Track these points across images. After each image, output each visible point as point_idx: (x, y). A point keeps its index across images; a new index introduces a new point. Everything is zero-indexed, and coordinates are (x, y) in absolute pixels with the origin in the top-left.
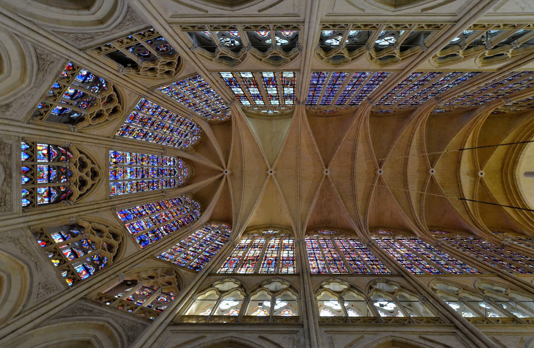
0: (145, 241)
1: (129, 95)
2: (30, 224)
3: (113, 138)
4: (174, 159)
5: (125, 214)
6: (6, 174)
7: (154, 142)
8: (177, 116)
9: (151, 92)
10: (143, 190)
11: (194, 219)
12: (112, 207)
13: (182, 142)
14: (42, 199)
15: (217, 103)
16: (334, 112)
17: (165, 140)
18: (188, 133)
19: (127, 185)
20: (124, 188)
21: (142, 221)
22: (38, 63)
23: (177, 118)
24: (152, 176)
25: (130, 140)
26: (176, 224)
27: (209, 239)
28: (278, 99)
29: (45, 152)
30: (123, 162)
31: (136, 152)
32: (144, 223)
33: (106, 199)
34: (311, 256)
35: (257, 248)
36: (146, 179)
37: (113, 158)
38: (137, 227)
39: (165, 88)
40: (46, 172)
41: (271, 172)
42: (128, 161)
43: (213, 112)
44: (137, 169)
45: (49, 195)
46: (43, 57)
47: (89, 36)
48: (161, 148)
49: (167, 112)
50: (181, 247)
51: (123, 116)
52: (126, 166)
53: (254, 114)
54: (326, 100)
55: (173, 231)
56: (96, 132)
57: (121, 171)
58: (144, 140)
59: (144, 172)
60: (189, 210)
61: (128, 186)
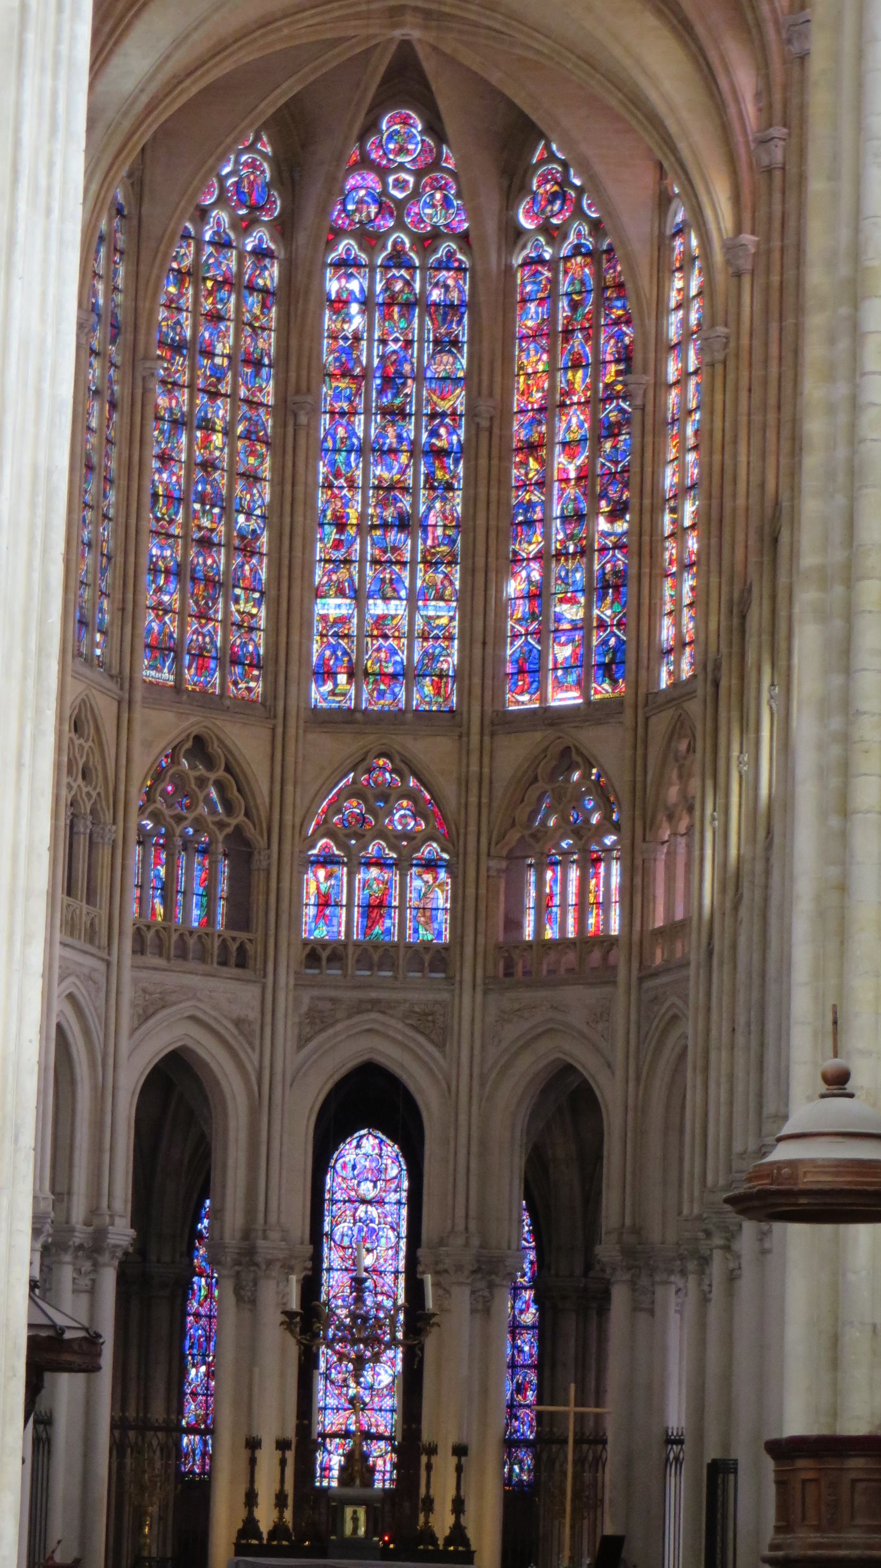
0: (615, 650)
2: (479, 980)
3: (275, 717)
5: (521, 671)
6: (371, 1011)
12: (487, 731)
14: (439, 886)
19: (428, 619)
20: (437, 638)
22: (153, 1014)
29: (321, 873)
32: (565, 606)
33: (460, 737)
37: (336, 685)
40: (374, 872)
42: (344, 611)
44: (375, 562)
45: (430, 865)
46: (141, 1012)
47: (90, 983)
48: (290, 429)
56: (261, 786)
57: (379, 650)
59: (389, 514)
61: (431, 613)
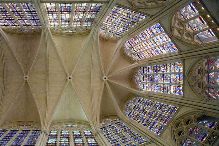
1: (167, 137)
4: (144, 88)
7: (156, 102)
8: (139, 122)
9: (152, 139)
10: (163, 65)
11: (129, 42)
13: (138, 102)
15: (109, 132)
16: (20, 125)
17: (149, 104)
18: (133, 109)
21: (161, 42)
23: (139, 120)
24: (158, 76)
25: (170, 103)
26: (140, 39)
27: (115, 27)
28: (61, 135)
30: (175, 87)
31: (167, 94)
33: (184, 59)
34: (35, 14)
35: (78, 20)
36: (161, 74)
37: (181, 90)
38: (164, 38)
39: (143, 143)
41: (70, 78)
43: (114, 125)
49: (145, 125)
50: (134, 22)
51: (172, 122)
52: (173, 84)
53: (83, 124)
54: (24, 134)
55: (141, 34)
58: (162, 104)
60: (133, 49)
